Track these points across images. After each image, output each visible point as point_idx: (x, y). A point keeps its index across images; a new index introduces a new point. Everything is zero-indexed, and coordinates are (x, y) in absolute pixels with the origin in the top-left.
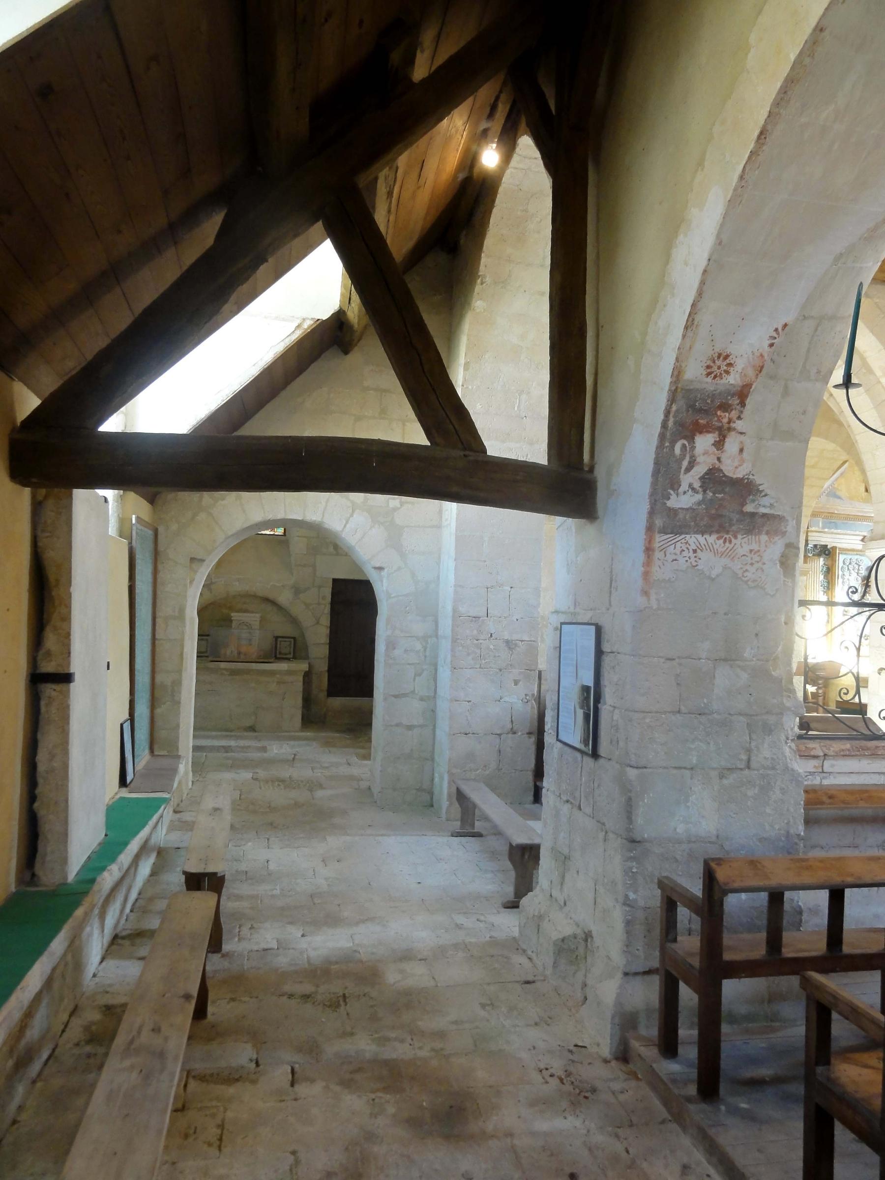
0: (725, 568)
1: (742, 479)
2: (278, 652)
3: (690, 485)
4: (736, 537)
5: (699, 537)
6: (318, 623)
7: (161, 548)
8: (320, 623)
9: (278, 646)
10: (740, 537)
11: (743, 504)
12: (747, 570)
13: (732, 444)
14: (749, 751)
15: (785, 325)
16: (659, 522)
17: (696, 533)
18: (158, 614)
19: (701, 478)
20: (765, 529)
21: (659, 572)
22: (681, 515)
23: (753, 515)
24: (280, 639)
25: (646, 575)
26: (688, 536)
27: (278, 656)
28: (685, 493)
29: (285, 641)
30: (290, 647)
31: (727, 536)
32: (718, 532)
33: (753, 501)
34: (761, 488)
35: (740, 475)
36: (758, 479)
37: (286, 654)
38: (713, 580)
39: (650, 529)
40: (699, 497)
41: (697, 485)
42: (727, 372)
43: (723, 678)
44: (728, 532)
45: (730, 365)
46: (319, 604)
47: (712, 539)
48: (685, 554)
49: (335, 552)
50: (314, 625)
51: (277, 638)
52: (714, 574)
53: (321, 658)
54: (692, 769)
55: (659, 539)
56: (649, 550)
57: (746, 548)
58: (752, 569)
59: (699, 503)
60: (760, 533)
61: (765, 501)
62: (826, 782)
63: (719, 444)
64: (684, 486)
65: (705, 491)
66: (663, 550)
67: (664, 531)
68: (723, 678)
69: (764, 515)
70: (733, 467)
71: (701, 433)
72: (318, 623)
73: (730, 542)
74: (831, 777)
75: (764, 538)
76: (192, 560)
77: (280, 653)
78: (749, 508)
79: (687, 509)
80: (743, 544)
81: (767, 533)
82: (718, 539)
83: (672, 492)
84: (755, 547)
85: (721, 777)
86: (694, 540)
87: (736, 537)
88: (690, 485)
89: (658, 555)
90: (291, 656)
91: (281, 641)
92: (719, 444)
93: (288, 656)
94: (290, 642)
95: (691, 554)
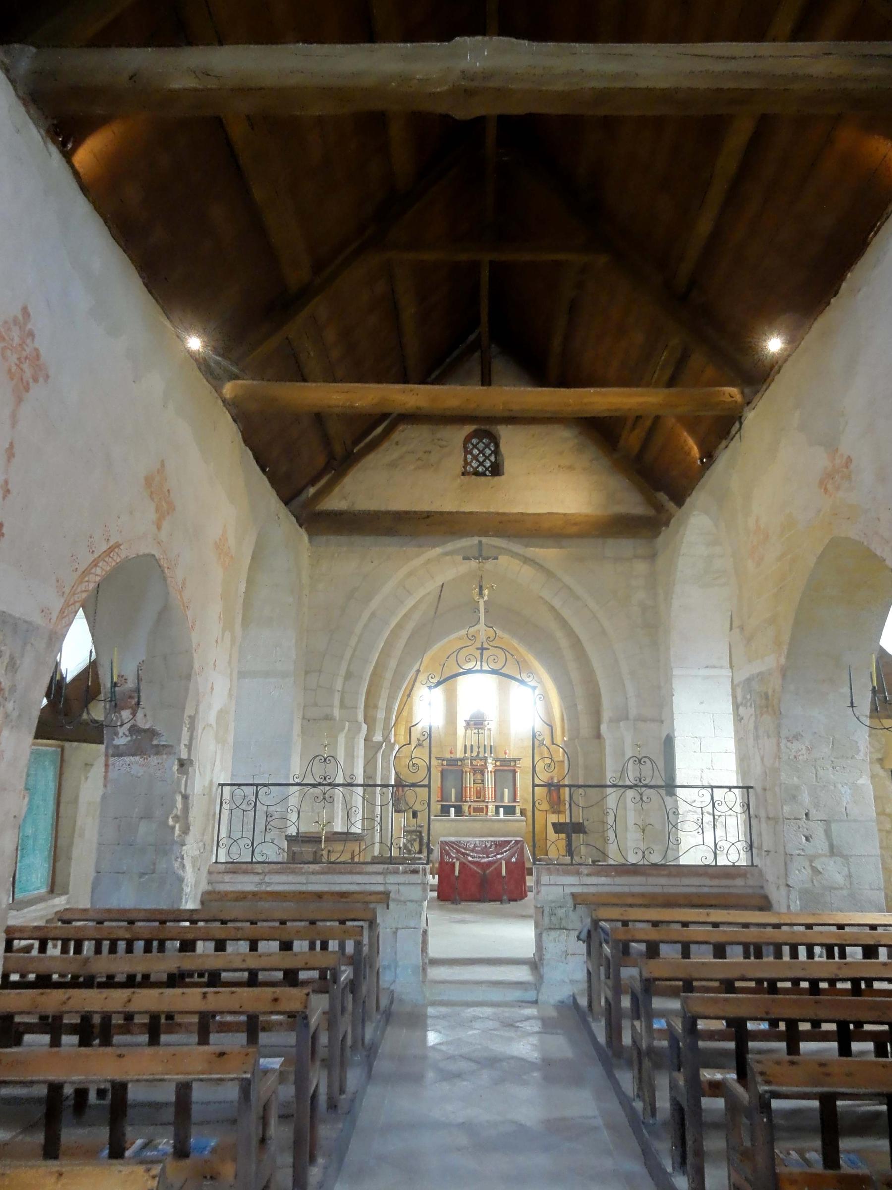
0: (144, 772)
1: (148, 729)
3: (124, 734)
4: (150, 757)
5: (131, 757)
7: (66, 757)
10: (152, 756)
11: (151, 740)
12: (157, 773)
13: (140, 714)
14: (154, 864)
15: (143, 661)
16: (110, 751)
17: (129, 756)
18: (63, 800)
19: (129, 730)
20: (164, 752)
21: (111, 775)
22: (121, 747)
23: (157, 746)
25: (105, 778)
26: (125, 758)
28: (122, 737)
31: (145, 756)
32: (140, 754)
33: (156, 739)
34: (159, 732)
35: (147, 728)
36: (157, 728)
38: (139, 778)
39: (106, 755)
40: (129, 739)
41: (127, 733)
42: (126, 682)
43: (143, 828)
44: (145, 754)
45: (126, 679)
47: (137, 758)
48: (124, 766)
52: (139, 775)
54: (124, 873)
55: (111, 760)
56: (106, 765)
57: (156, 762)
58: (160, 772)
59: (129, 741)
60: (162, 754)
61: (163, 738)
62: (268, 889)
63: (134, 714)
64: (121, 734)
65: (131, 736)
66: (113, 764)
67: (113, 756)
68: (143, 828)
69: (163, 746)
70: (142, 722)
71: (123, 709)
73: (147, 759)
74: (272, 885)
75: (164, 756)
76: (86, 764)
78: (155, 742)
79: (124, 745)
80: (153, 760)
81: (166, 754)
82: (141, 758)
83: (115, 737)
84: (160, 761)
85: (140, 877)
86: (128, 759)
87: (150, 757)
88: (124, 734)
89: (111, 767)
92: (134, 714)
95: (127, 766)
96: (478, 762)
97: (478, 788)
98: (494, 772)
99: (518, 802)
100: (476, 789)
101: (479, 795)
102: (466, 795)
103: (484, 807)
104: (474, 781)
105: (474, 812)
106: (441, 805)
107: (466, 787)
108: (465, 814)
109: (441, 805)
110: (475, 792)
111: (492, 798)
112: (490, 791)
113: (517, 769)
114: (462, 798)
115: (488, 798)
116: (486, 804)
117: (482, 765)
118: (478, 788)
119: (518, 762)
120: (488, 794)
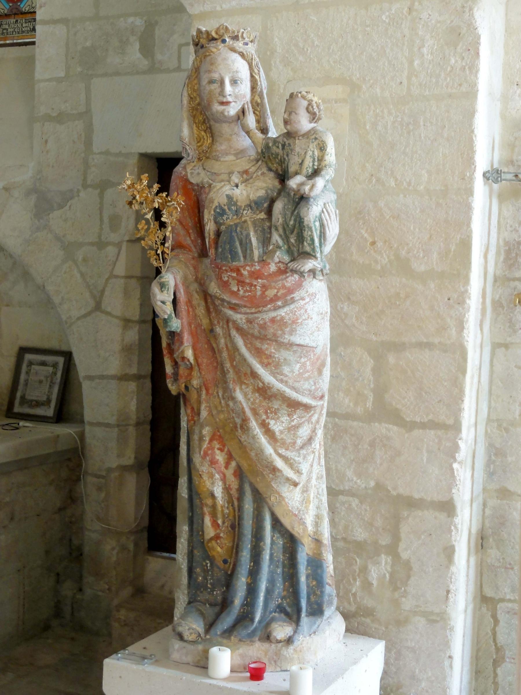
2: (19, 394)
6: (98, 307)
8: (103, 307)
9: (23, 377)
24: (28, 357)
27: (17, 409)
29: (43, 364)
30: (52, 383)
37: (38, 404)
46: (101, 245)
49: (145, 63)
50: (89, 314)
51: (23, 351)
53: (108, 425)
72: (98, 307)
77: (24, 401)
90: (50, 412)
91: (31, 363)
93: (40, 411)
94: (55, 365)
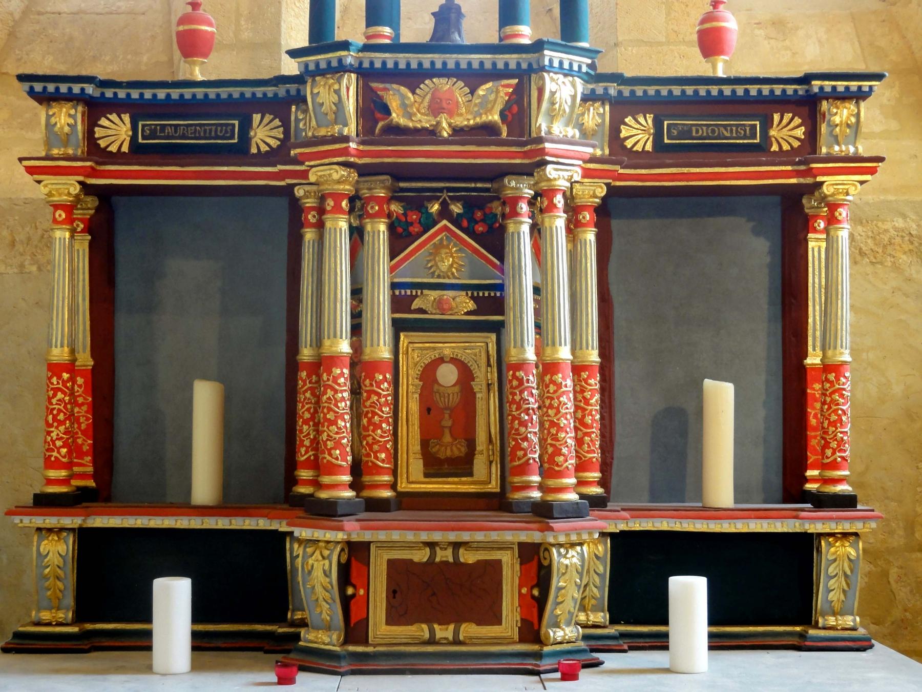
96: (435, 109)
97: (448, 375)
98: (603, 211)
99: (848, 502)
100: (428, 374)
101: (450, 447)
102: (316, 444)
103: (510, 565)
104: (399, 303)
105: (395, 617)
106: (84, 536)
107: (323, 363)
108: (311, 638)
109: (84, 536)
110: (411, 406)
111: (581, 467)
112: (568, 402)
113: (831, 184)
114: (291, 480)
115: (549, 470)
116: (535, 537)
117: (489, 130)
118: (448, 375)
119: (841, 114)
120: (549, 429)
